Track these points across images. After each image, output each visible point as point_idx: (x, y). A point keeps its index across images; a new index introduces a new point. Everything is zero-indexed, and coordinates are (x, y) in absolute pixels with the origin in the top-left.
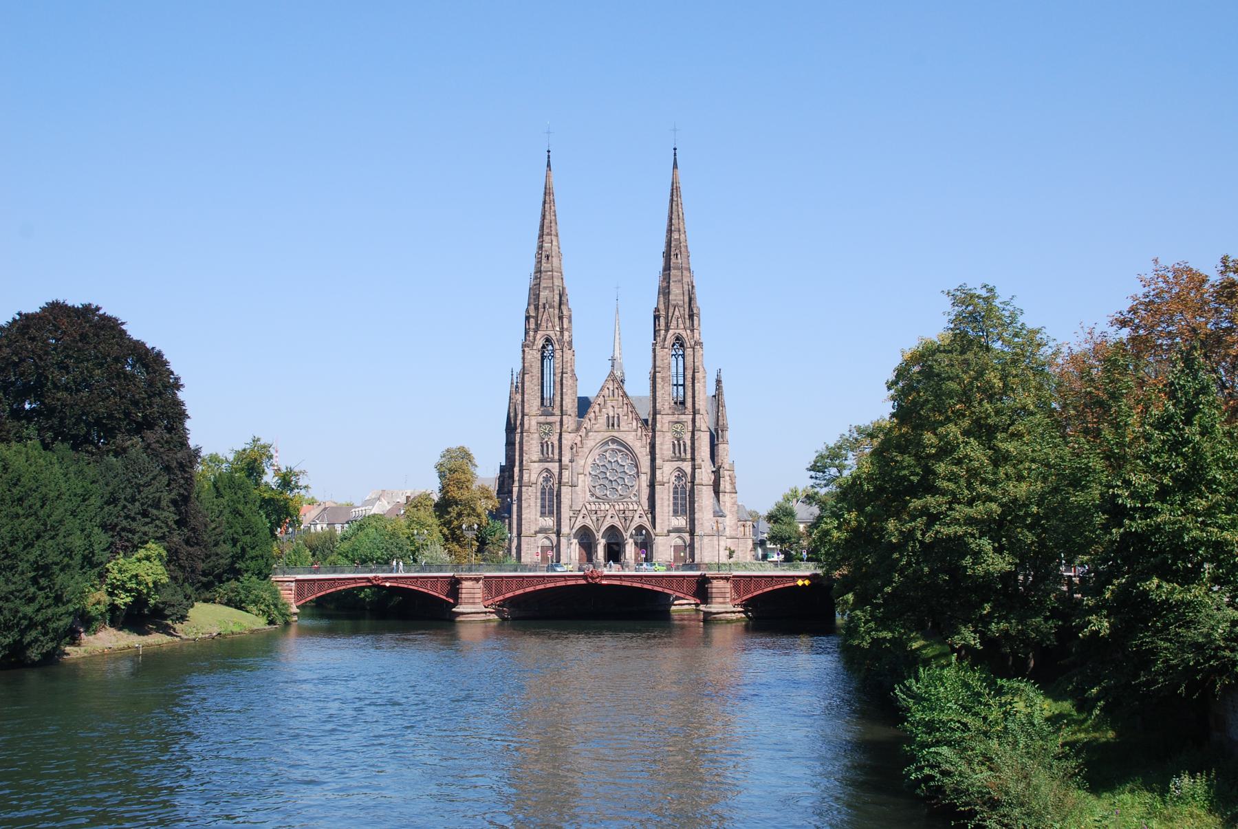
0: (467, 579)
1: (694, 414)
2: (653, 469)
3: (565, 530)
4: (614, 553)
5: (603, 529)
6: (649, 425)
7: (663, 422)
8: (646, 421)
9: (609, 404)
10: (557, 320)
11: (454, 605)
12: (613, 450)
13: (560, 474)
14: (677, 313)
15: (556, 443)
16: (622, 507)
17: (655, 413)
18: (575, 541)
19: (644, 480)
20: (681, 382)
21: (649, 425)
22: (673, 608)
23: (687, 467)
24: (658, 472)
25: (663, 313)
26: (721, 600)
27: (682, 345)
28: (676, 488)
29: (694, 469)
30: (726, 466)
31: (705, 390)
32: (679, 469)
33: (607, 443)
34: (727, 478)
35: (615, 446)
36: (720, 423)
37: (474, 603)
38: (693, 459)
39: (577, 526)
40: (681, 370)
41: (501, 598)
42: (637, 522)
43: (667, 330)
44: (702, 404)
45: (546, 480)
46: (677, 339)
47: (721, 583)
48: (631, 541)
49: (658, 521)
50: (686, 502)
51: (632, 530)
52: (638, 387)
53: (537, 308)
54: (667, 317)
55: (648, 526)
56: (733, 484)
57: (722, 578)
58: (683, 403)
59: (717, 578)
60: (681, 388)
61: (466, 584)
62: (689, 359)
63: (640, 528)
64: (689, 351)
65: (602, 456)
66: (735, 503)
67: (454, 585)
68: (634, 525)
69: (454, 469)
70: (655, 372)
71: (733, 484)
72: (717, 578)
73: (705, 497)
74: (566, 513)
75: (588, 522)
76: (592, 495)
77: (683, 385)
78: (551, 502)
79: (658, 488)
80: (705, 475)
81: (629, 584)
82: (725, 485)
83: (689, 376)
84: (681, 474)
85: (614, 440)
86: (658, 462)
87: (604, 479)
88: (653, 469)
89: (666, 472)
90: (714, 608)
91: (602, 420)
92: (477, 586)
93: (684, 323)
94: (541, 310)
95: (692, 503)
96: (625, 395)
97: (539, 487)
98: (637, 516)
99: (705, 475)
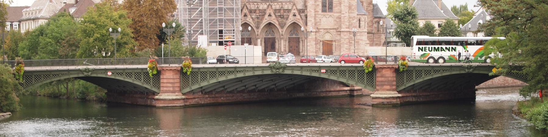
5: (262, 26)
11: (154, 93)
16: (278, 7)
37: (174, 92)
68: (289, 22)
81: (308, 74)
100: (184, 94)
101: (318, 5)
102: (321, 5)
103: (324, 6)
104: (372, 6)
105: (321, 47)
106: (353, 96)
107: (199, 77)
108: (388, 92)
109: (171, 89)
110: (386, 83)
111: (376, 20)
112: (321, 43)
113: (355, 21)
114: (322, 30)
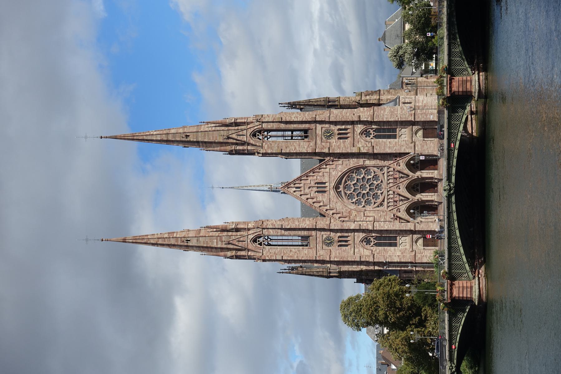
0: (451, 293)
1: (316, 122)
2: (359, 155)
3: (410, 226)
4: (429, 185)
6: (324, 157)
7: (322, 147)
8: (321, 161)
9: (307, 191)
10: (239, 233)
12: (345, 188)
13: (363, 231)
14: (234, 136)
15: (339, 234)
17: (315, 154)
18: (419, 219)
19: (368, 162)
20: (290, 133)
21: (324, 157)
22: (474, 134)
23: (359, 128)
24: (363, 150)
25: (233, 147)
26: (468, 84)
27: (260, 132)
28: (376, 137)
29: (360, 122)
30: (358, 98)
31: (296, 115)
32: (361, 133)
33: (339, 193)
34: (368, 97)
35: (341, 186)
36: (323, 103)
37: (471, 287)
38: (353, 123)
39: (407, 217)
40: (280, 133)
41: (467, 265)
42: (402, 167)
43: (249, 144)
44: (307, 116)
45: (368, 242)
46: (254, 135)
47: (455, 84)
48: (418, 174)
49: (402, 151)
50: (387, 129)
51: (411, 174)
52: (295, 167)
53: (229, 249)
54: (237, 144)
55: (407, 158)
56: (372, 93)
57: (451, 83)
58: (306, 131)
59: (451, 87)
60: (295, 133)
61: (455, 294)
62: (270, 126)
63: (408, 165)
64: (265, 126)
65: (350, 197)
66: (388, 92)
67: (456, 305)
68: (407, 171)
69: (358, 315)
70: (282, 154)
71: (372, 93)
72: (451, 87)
73: (385, 114)
74: (397, 226)
75: (403, 207)
76: (381, 204)
77: (292, 131)
78: (387, 238)
79: (375, 151)
80: (365, 114)
81: (455, 160)
82: (373, 99)
83: (283, 126)
84: (365, 133)
85: (337, 187)
86: (355, 150)
87: (366, 194)
88: (359, 155)
89: (363, 145)
90: (475, 89)
91: (320, 197)
92: (457, 285)
93: (242, 130)
94: (231, 246)
95: (388, 123)
96: (300, 179)
97: (374, 248)
98: (398, 168)
99: (365, 114)
100: (474, 277)
101: (390, 142)
102: (389, 140)
103: (389, 137)
104: (391, 91)
105: (430, 139)
106: (477, 111)
107: (458, 263)
108: (473, 84)
109: (469, 290)
110: (465, 86)
111: (404, 86)
112: (425, 139)
113: (405, 108)
114: (413, 139)
